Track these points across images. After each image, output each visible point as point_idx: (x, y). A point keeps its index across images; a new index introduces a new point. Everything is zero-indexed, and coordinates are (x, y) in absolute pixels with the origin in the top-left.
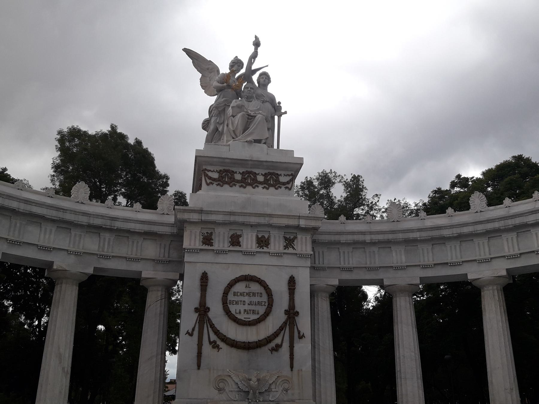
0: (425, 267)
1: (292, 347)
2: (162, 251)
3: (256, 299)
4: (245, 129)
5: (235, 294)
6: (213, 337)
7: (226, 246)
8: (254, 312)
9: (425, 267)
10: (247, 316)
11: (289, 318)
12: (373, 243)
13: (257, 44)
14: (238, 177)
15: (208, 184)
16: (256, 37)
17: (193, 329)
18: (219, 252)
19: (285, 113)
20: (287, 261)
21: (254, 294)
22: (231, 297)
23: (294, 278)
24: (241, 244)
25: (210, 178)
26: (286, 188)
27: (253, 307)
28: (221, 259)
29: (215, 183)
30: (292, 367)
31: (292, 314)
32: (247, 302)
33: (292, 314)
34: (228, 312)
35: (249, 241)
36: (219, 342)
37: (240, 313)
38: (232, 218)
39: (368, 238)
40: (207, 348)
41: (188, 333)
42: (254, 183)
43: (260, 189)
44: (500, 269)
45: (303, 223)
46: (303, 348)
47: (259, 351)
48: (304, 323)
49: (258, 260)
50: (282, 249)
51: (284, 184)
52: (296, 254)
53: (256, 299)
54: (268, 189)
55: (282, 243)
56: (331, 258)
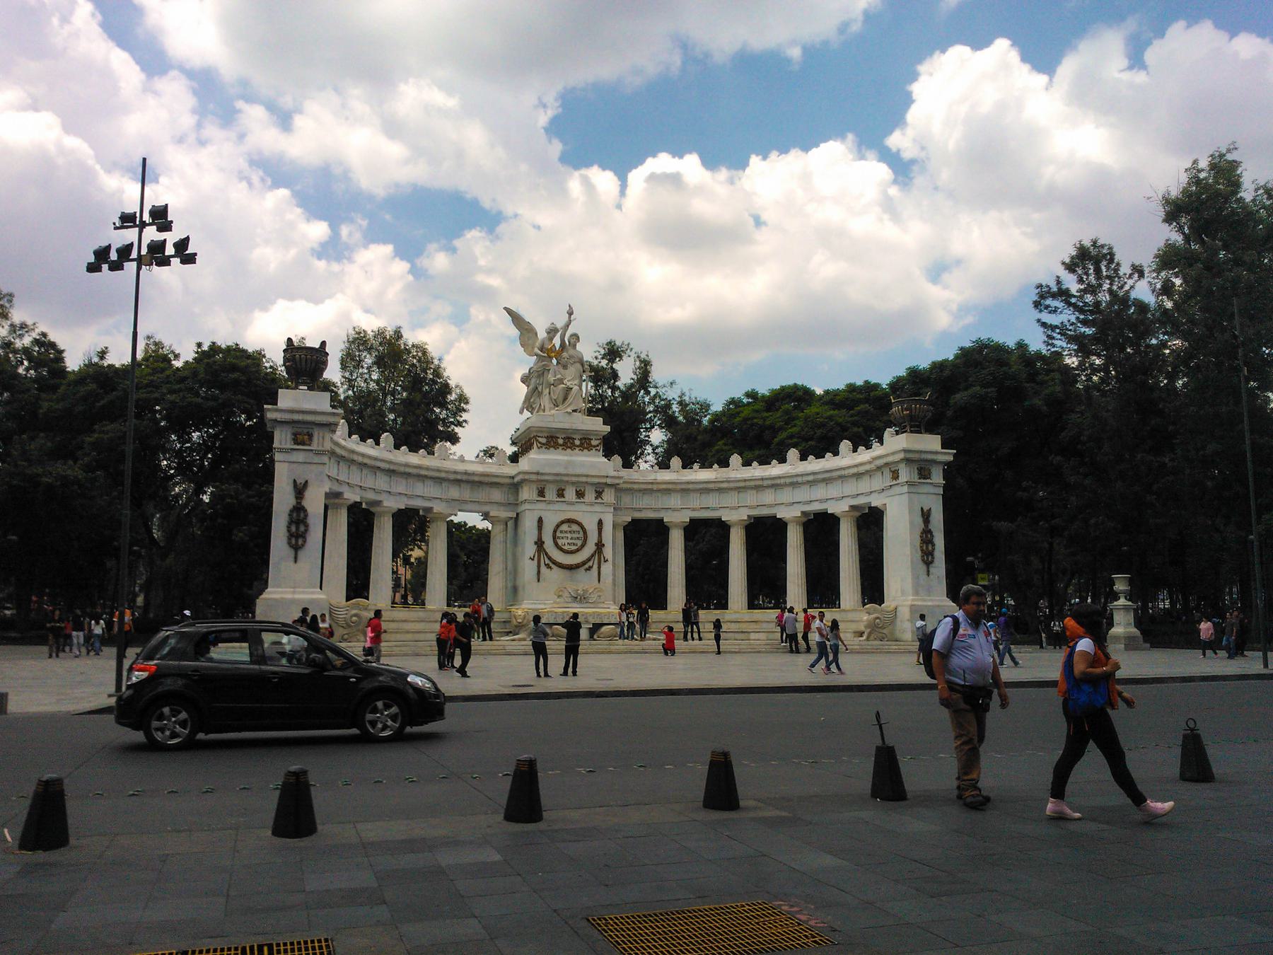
0: (694, 510)
1: (599, 568)
3: (575, 535)
4: (565, 399)
7: (555, 498)
9: (694, 510)
12: (659, 491)
13: (570, 313)
14: (561, 441)
18: (550, 502)
20: (598, 508)
22: (558, 534)
28: (551, 507)
31: (600, 545)
33: (600, 545)
34: (556, 544)
35: (570, 494)
38: (558, 478)
39: (655, 487)
42: (573, 447)
43: (577, 451)
44: (743, 515)
45: (609, 481)
49: (578, 507)
50: (593, 500)
53: (575, 535)
55: (594, 495)
56: (626, 500)
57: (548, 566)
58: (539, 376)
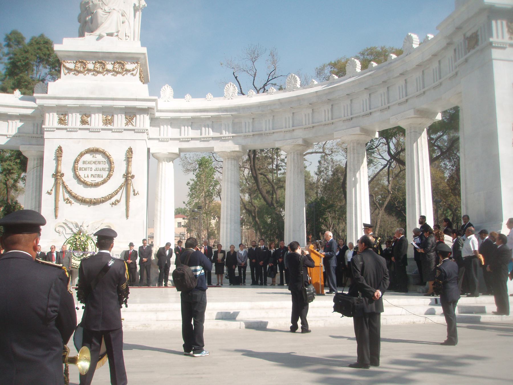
2: (36, 129)
5: (84, 162)
6: (67, 196)
8: (99, 176)
10: (93, 179)
11: (127, 180)
15: (65, 75)
17: (52, 190)
21: (99, 163)
22: (80, 165)
23: (131, 149)
24: (89, 123)
25: (68, 69)
26: (132, 74)
27: (98, 173)
28: (73, 135)
30: (127, 216)
31: (128, 177)
32: (94, 168)
33: (128, 177)
36: (71, 199)
37: (88, 177)
40: (61, 203)
41: (48, 192)
46: (139, 203)
47: (101, 205)
48: (140, 183)
51: (129, 71)
52: (134, 130)
54: (116, 76)
55: (124, 121)
57: (67, 201)
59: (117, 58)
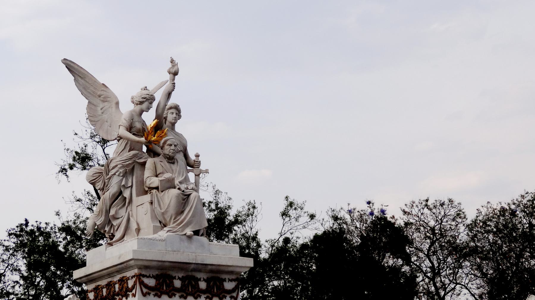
16: (172, 61)
19: (207, 172)
25: (146, 286)
29: (152, 293)
58: (125, 175)
59: (211, 271)
